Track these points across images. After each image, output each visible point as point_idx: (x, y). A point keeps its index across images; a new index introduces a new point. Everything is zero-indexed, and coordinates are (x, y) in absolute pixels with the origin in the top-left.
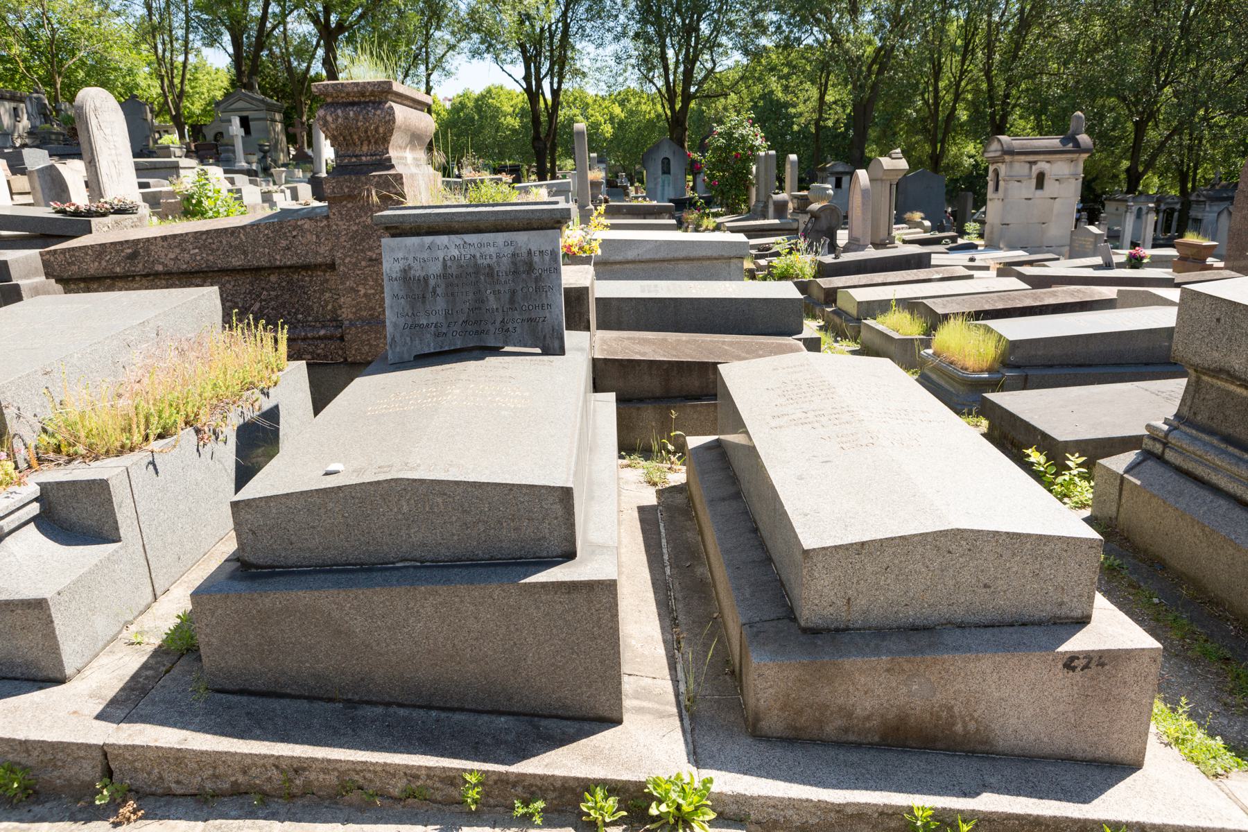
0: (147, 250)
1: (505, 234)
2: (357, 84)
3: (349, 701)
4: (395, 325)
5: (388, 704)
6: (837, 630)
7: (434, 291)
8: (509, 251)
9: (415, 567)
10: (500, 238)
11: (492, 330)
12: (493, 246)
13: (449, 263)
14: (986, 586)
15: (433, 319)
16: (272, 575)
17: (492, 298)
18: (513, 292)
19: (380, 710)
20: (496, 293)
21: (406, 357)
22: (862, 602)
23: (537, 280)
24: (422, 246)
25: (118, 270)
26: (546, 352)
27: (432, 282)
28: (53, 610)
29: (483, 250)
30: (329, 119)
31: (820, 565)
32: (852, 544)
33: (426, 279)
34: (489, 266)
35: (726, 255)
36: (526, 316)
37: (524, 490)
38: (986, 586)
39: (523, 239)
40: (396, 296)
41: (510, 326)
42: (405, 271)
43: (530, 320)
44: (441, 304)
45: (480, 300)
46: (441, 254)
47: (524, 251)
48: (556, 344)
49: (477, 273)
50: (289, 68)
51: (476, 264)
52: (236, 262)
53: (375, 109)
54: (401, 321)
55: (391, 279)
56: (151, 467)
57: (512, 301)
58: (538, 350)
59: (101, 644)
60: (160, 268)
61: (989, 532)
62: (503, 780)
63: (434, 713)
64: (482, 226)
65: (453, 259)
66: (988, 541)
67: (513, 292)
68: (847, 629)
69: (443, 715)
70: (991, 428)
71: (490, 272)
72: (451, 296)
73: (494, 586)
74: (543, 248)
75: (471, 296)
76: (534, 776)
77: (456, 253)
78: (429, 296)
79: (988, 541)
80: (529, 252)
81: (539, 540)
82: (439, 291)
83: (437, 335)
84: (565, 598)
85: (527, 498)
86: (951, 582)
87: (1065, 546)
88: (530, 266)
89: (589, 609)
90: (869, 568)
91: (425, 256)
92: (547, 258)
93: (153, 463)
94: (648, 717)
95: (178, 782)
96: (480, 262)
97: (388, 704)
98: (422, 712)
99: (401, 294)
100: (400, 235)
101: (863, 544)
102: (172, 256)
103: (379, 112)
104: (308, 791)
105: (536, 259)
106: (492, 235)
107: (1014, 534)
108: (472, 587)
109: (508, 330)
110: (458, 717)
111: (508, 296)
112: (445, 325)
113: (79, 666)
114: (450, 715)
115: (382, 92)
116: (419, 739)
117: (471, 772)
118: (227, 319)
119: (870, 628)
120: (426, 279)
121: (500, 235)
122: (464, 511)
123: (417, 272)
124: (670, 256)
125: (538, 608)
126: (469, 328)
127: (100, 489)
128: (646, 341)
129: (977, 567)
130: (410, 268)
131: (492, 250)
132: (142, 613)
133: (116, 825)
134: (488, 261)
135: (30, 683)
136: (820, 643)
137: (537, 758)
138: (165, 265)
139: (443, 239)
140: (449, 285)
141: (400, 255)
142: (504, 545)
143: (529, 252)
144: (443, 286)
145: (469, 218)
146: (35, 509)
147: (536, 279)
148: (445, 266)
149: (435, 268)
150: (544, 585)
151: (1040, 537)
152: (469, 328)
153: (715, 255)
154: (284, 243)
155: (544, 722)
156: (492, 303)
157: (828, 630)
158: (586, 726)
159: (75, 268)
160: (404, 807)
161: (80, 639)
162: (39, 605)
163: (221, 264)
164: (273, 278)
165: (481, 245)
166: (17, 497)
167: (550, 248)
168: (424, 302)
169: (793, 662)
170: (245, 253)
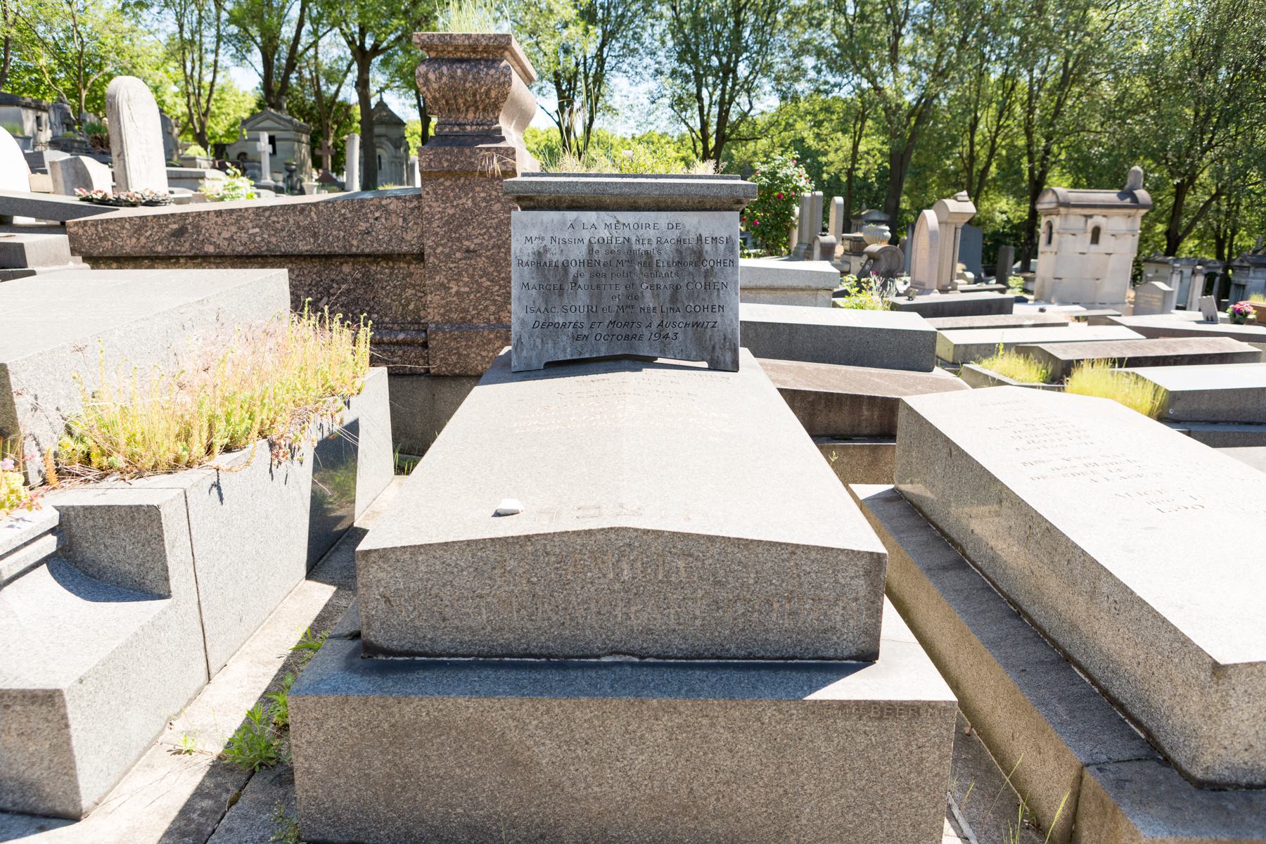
0: (197, 227)
4: (523, 323)
6: (1250, 787)
8: (675, 234)
9: (632, 665)
10: (664, 218)
11: (647, 334)
13: (596, 247)
15: (572, 318)
17: (648, 294)
18: (676, 288)
21: (535, 364)
25: (159, 249)
26: (714, 367)
27: (573, 270)
29: (640, 232)
30: (432, 76)
31: (1240, 689)
34: (647, 253)
35: (813, 285)
36: (691, 320)
41: (670, 331)
44: (582, 298)
45: (633, 297)
46: (586, 236)
47: (692, 236)
48: (729, 357)
49: (631, 261)
50: (318, 93)
51: (630, 250)
52: (303, 247)
53: (489, 68)
54: (531, 318)
55: (520, 263)
56: (215, 490)
57: (674, 298)
58: (705, 365)
59: (134, 753)
60: (210, 249)
64: (641, 203)
65: (602, 241)
67: (676, 288)
71: (648, 261)
72: (596, 289)
73: (765, 703)
75: (622, 290)
77: (605, 234)
78: (568, 287)
80: (699, 238)
81: (825, 632)
82: (581, 281)
83: (576, 338)
84: (872, 726)
85: (815, 567)
88: (699, 257)
89: (908, 745)
92: (722, 247)
93: (217, 485)
96: (635, 247)
99: (532, 282)
100: (533, 208)
102: (226, 235)
103: (492, 72)
105: (708, 247)
106: (652, 214)
109: (666, 336)
111: (669, 292)
112: (587, 325)
118: (296, 306)
120: (566, 265)
123: (555, 256)
124: (752, 284)
125: (829, 739)
126: (617, 331)
127: (146, 520)
128: (782, 368)
130: (546, 251)
131: (652, 234)
132: (190, 701)
134: (647, 247)
135: (25, 820)
138: (218, 246)
139: (590, 217)
142: (771, 636)
143: (699, 238)
144: (587, 276)
145: (626, 190)
147: (706, 272)
148: (590, 250)
149: (578, 253)
150: (842, 706)
152: (617, 331)
153: (802, 285)
154: (363, 226)
156: (649, 301)
157: (1237, 786)
159: (107, 244)
162: (50, 699)
163: (284, 247)
164: (346, 269)
165: (638, 226)
166: (25, 527)
167: (725, 235)
168: (561, 295)
170: (315, 235)
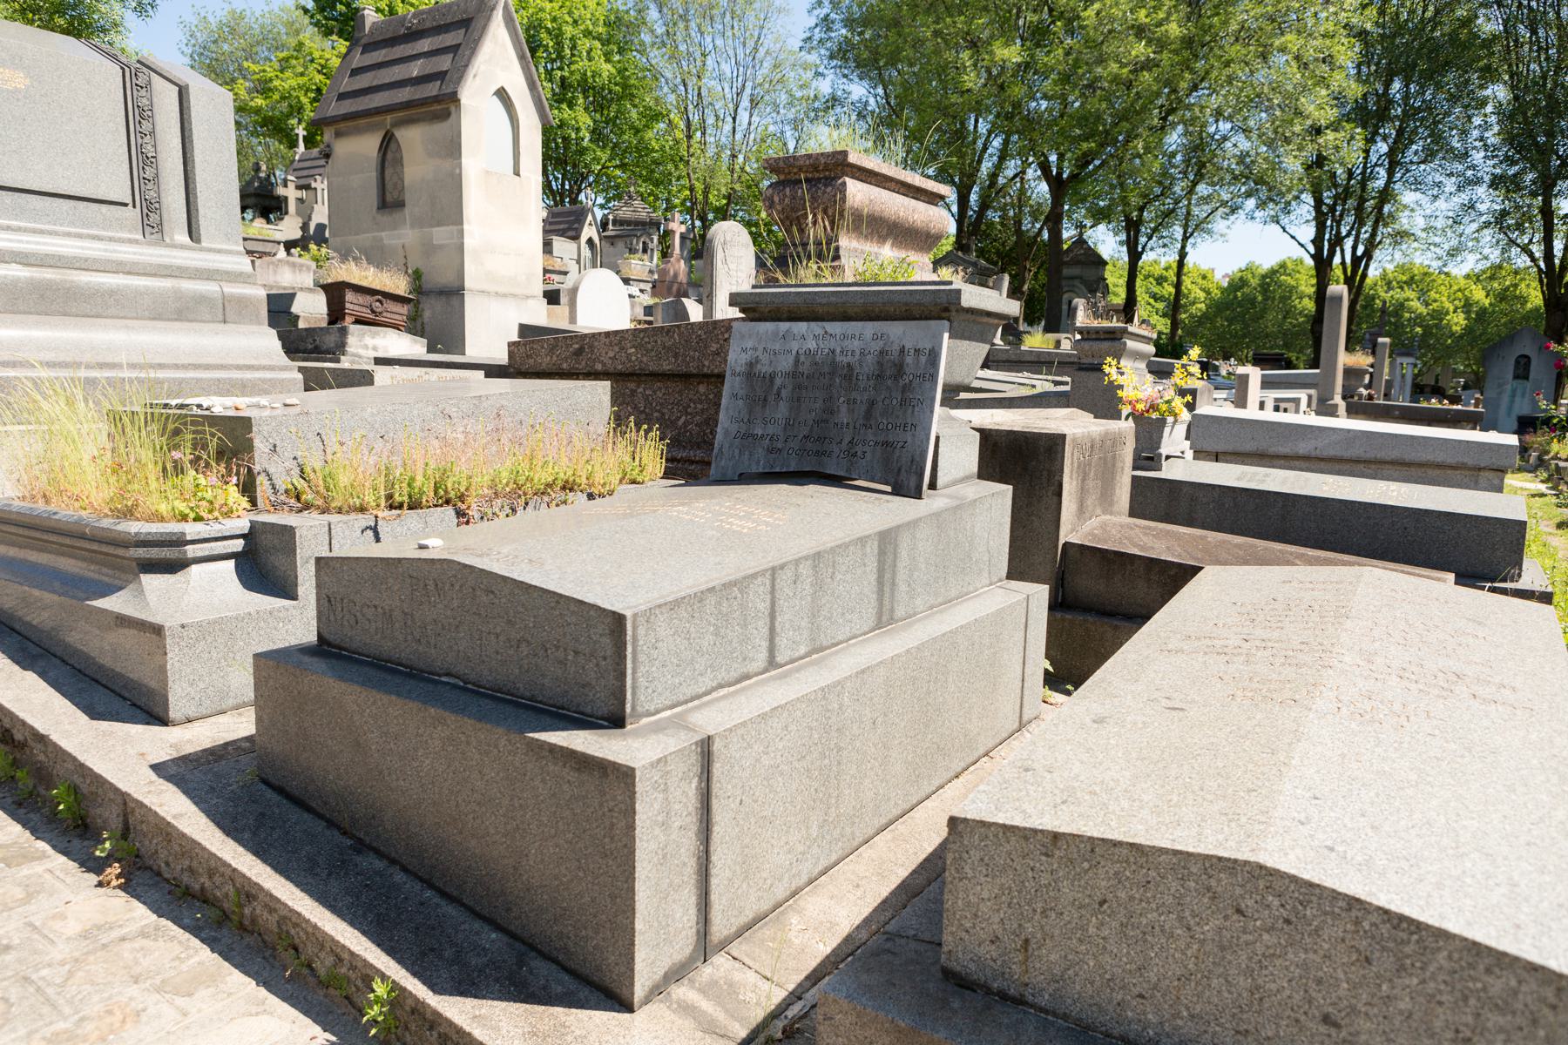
0: (591, 347)
1: (876, 323)
2: (809, 156)
3: (360, 841)
4: (727, 432)
5: (393, 862)
6: (1004, 996)
7: (778, 394)
8: (876, 346)
9: (455, 686)
10: (869, 328)
11: (836, 451)
12: (858, 338)
13: (802, 358)
14: (1326, 1019)
15: (771, 430)
16: (339, 657)
17: (844, 409)
18: (872, 403)
19: (379, 864)
20: (851, 402)
21: (730, 475)
22: (1050, 957)
23: (905, 389)
24: (776, 334)
25: (565, 366)
26: (898, 491)
27: (778, 381)
28: (168, 641)
29: (846, 343)
30: (776, 199)
31: (976, 855)
32: (1035, 831)
33: (772, 377)
34: (849, 365)
35: (1470, 462)
36: (881, 438)
37: (573, 607)
38: (1326, 1019)
39: (898, 332)
40: (735, 396)
41: (859, 449)
42: (751, 365)
43: (886, 444)
44: (782, 411)
45: (830, 411)
46: (795, 346)
47: (896, 347)
48: (912, 484)
49: (832, 374)
50: (1019, 232)
51: (834, 361)
52: (666, 366)
53: (826, 186)
54: (734, 428)
55: (734, 374)
56: (370, 533)
57: (868, 414)
58: (889, 489)
59: (231, 702)
60: (599, 367)
61: (1336, 895)
62: (419, 1009)
63: (428, 893)
64: (850, 312)
65: (808, 353)
66: (1335, 916)
67: (872, 403)
68: (1019, 1001)
69: (437, 900)
70: (296, 325)
71: (849, 374)
72: (796, 401)
73: (500, 730)
74: (920, 346)
75: (819, 404)
76: (450, 1023)
77: (812, 345)
78: (771, 398)
79: (1335, 916)
80: (902, 350)
81: (584, 686)
82: (784, 393)
83: (770, 451)
84: (573, 776)
85: (574, 619)
86: (1243, 983)
87: (1549, 993)
88: (899, 368)
89: (601, 805)
90: (1068, 892)
91: (777, 347)
92: (923, 359)
93: (375, 530)
94: (688, 1024)
95: (167, 864)
96: (839, 359)
97: (393, 862)
98: (418, 886)
99: (742, 393)
100: (760, 320)
101: (1056, 837)
102: (611, 354)
103: (829, 189)
104: (246, 928)
105: (909, 360)
106: (860, 324)
107: (1402, 918)
108: (479, 725)
109: (855, 455)
110: (450, 910)
111: (864, 408)
112: (782, 438)
113: (192, 714)
114: (443, 903)
115: (837, 165)
116: (379, 915)
117: (384, 977)
118: (619, 420)
119: (1065, 1017)
120: (772, 377)
121: (870, 324)
122: (509, 622)
123: (764, 368)
124: (1370, 455)
125: (543, 781)
126: (809, 445)
127: (289, 532)
129: (1305, 966)
130: (757, 360)
131: (856, 345)
133: (100, 884)
134: (849, 358)
135: (144, 716)
136: (956, 1004)
137: (476, 1002)
138: (604, 365)
139: (801, 327)
140: (798, 387)
141: (750, 344)
142: (546, 681)
143: (902, 350)
144: (790, 387)
145: (833, 299)
146: (238, 545)
147: (904, 387)
148: (797, 361)
149: (785, 364)
150: (553, 749)
151: (1475, 948)
152: (809, 445)
153: (1450, 460)
154: (714, 347)
155: (538, 964)
156: (843, 416)
157: (988, 991)
158: (584, 992)
159: (531, 361)
160: (326, 996)
161: (202, 685)
162: (158, 630)
163: (652, 367)
164: (702, 388)
165: (845, 337)
166: (217, 526)
167: (928, 346)
168: (764, 406)
169: (881, 1014)
170: (676, 356)
